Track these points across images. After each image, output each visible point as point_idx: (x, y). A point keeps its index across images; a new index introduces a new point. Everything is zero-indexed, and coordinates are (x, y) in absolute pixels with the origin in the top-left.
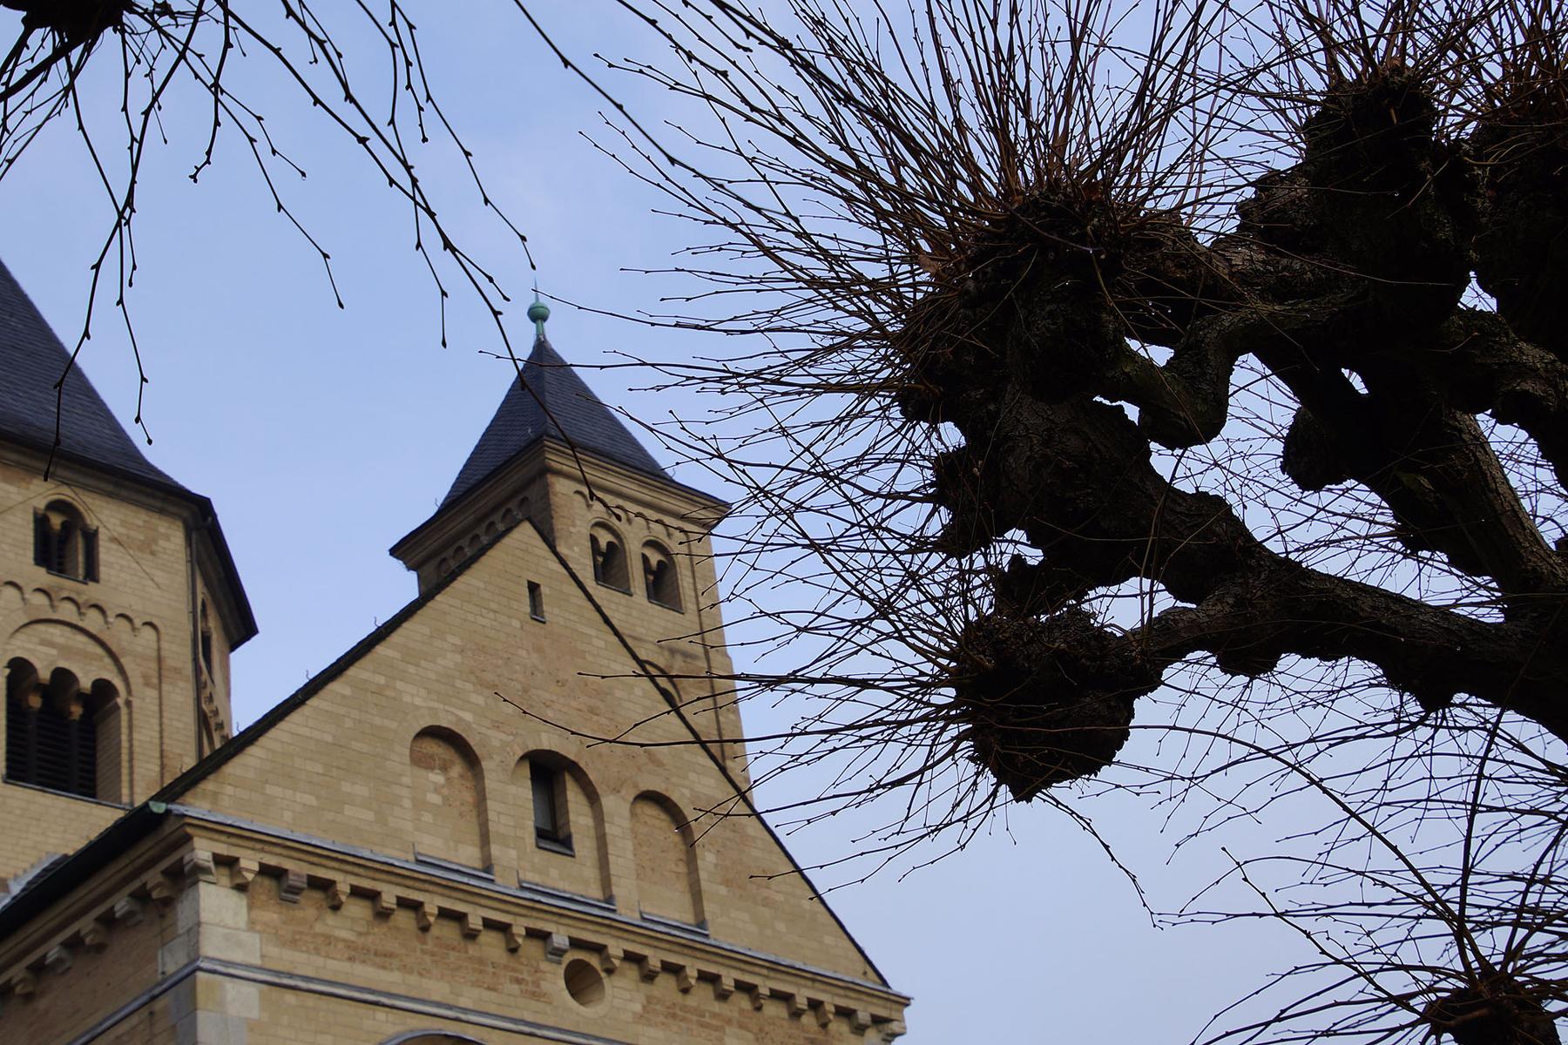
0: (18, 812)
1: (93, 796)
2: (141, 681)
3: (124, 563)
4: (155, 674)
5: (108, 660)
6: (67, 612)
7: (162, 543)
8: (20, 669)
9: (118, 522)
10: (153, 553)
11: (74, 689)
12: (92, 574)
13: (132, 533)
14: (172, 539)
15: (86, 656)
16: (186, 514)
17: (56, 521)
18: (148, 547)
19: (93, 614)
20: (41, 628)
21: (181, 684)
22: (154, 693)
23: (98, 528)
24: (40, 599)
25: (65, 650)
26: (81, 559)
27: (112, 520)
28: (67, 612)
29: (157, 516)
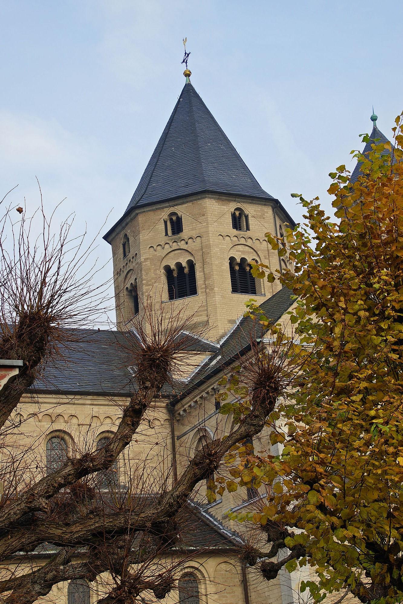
0: (236, 301)
1: (255, 293)
2: (264, 258)
3: (256, 223)
4: (267, 255)
5: (255, 253)
6: (242, 241)
7: (266, 214)
8: (232, 259)
9: (253, 211)
10: (264, 218)
11: (247, 263)
12: (248, 229)
13: (257, 213)
14: (268, 212)
15: (249, 253)
16: (272, 204)
17: (237, 213)
18: (262, 217)
19: (250, 240)
20: (236, 247)
21: (275, 257)
22: (268, 261)
23: (248, 215)
24: (235, 239)
25: (243, 252)
26: (245, 223)
27: (252, 211)
28: (242, 241)
29: (264, 206)
